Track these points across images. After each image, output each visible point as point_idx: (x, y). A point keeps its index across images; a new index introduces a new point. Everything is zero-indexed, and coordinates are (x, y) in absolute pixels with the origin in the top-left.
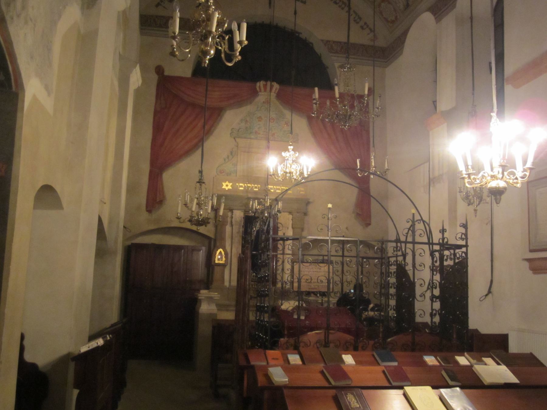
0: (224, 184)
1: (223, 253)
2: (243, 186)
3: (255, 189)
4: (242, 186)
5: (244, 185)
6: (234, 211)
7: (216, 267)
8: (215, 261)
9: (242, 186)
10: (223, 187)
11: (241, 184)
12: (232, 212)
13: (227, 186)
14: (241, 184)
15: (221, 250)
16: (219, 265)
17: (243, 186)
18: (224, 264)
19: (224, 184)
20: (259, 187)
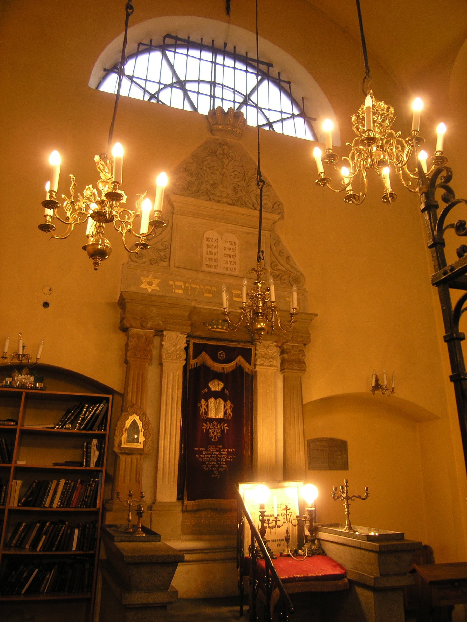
0: (144, 279)
1: (140, 424)
2: (183, 287)
3: (207, 295)
4: (179, 287)
5: (185, 285)
6: (165, 333)
7: (122, 458)
8: (121, 443)
9: (179, 287)
10: (142, 286)
11: (177, 283)
12: (162, 336)
13: (150, 284)
14: (177, 283)
15: (137, 418)
16: (131, 452)
17: (183, 287)
18: (143, 449)
19: (144, 279)
20: (214, 291)
